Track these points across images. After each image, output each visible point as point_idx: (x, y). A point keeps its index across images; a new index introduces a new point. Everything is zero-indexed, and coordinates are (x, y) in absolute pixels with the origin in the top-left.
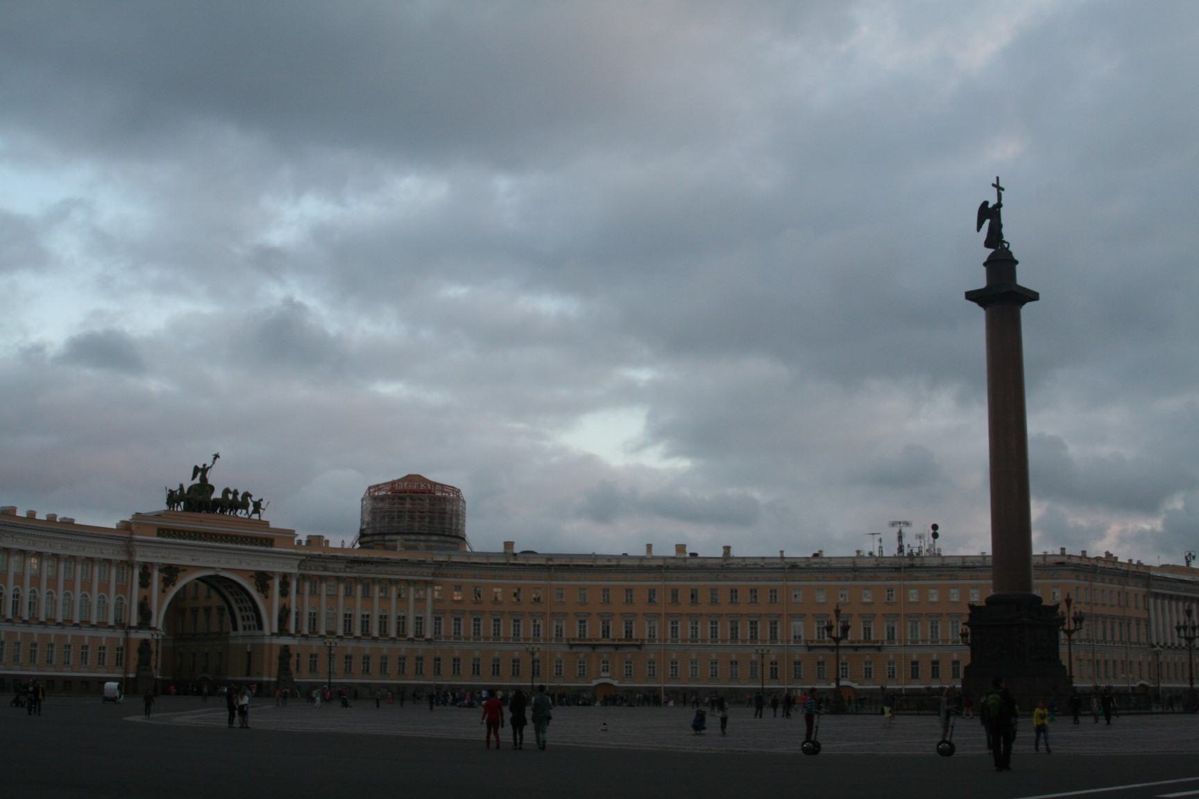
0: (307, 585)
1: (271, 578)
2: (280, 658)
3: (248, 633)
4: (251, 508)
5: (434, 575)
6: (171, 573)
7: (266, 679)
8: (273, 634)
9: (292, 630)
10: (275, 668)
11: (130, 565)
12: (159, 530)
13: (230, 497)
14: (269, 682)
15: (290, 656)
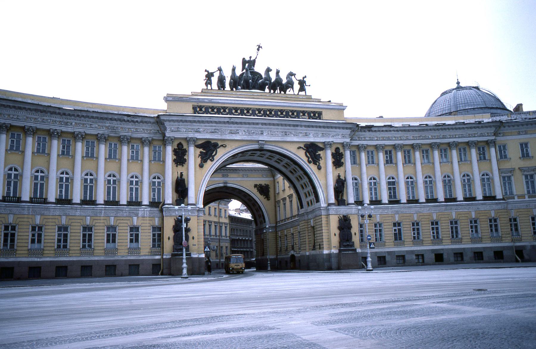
0: (363, 156)
1: (322, 149)
2: (340, 228)
3: (311, 208)
4: (297, 86)
5: (495, 134)
6: (208, 149)
7: (326, 252)
8: (329, 205)
9: (351, 200)
10: (335, 240)
11: (164, 141)
12: (194, 108)
13: (273, 77)
14: (329, 255)
15: (350, 227)
